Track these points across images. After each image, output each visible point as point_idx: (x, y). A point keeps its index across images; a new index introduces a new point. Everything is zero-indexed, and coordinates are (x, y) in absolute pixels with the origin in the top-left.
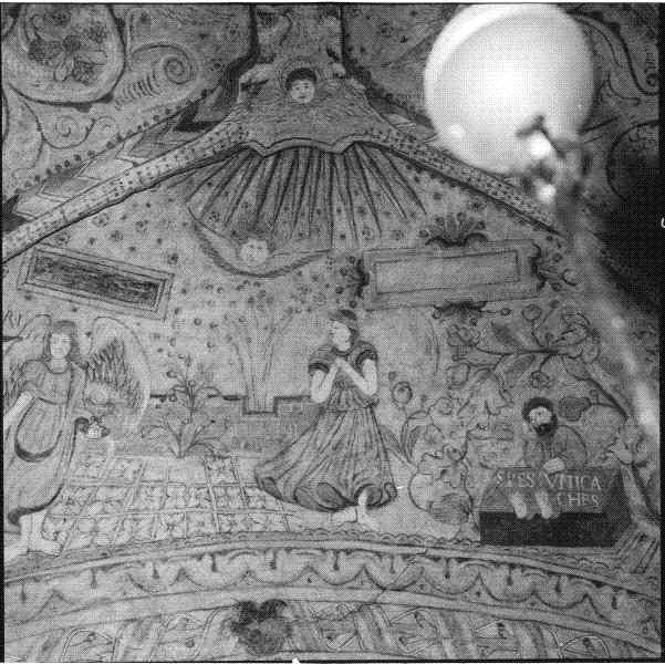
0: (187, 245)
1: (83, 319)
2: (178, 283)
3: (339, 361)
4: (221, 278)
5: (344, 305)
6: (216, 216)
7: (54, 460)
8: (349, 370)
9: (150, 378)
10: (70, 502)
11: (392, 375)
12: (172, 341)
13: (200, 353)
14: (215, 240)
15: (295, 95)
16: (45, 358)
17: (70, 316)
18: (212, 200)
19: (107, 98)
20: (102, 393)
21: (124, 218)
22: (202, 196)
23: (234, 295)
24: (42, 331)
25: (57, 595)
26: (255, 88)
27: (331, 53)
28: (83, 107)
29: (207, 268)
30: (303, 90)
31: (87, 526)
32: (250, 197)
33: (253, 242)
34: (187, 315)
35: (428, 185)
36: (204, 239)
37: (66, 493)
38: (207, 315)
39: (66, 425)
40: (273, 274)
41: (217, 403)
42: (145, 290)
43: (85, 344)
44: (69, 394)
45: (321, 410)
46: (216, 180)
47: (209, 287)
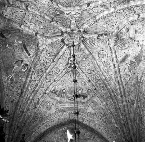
1: (127, 62)
2: (127, 53)
3: (138, 44)
5: (134, 40)
8: (140, 44)
9: (134, 60)
10: (139, 73)
11: (141, 41)
12: (132, 56)
15: (110, 41)
16: (129, 67)
18: (120, 47)
20: (133, 64)
21: (119, 56)
22: (119, 48)
23: (130, 49)
24: (126, 66)
27: (107, 37)
29: (126, 50)
30: (110, 40)
31: (140, 74)
35: (122, 31)
36: (124, 49)
37: (138, 73)
38: (131, 52)
39: (134, 69)
42: (127, 56)
43: (129, 63)
44: (132, 67)
45: (142, 49)
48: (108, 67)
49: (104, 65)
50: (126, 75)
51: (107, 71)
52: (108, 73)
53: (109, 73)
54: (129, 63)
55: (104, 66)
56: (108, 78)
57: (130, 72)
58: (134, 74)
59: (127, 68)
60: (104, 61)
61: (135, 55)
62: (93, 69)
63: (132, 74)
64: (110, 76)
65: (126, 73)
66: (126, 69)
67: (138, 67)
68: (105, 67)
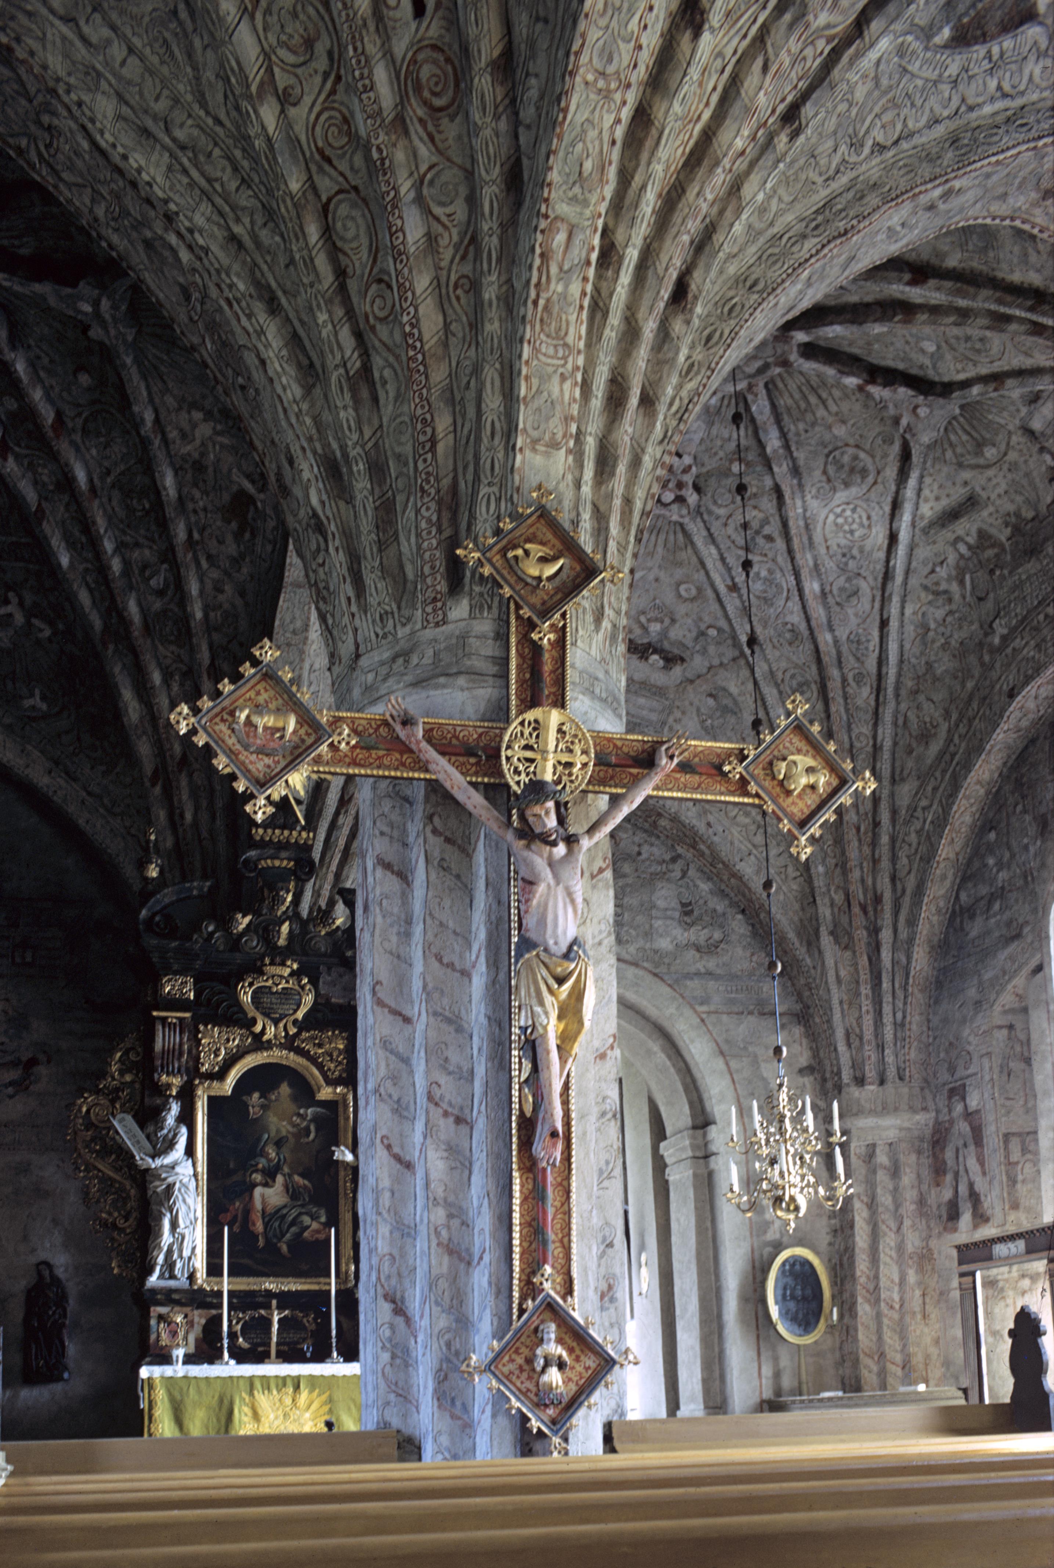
0: (966, 475)
4: (990, 473)
6: (962, 455)
7: (992, 595)
9: (1003, 535)
13: (1011, 508)
14: (973, 462)
17: (954, 537)
19: (878, 473)
20: (990, 553)
25: (1014, 649)
26: (909, 428)
28: (875, 483)
32: (965, 437)
33: (985, 450)
34: (993, 496)
40: (1005, 454)
41: (1029, 526)
43: (970, 540)
46: (946, 446)
47: (990, 480)
48: (857, 534)
49: (840, 520)
50: (936, 593)
51: (844, 555)
52: (846, 564)
53: (852, 564)
54: (971, 540)
55: (836, 525)
56: (835, 592)
57: (962, 583)
58: (980, 599)
59: (952, 558)
60: (844, 499)
61: (1018, 515)
62: (767, 530)
63: (964, 597)
64: (849, 580)
65: (937, 584)
66: (942, 563)
67: (1010, 573)
68: (841, 534)
